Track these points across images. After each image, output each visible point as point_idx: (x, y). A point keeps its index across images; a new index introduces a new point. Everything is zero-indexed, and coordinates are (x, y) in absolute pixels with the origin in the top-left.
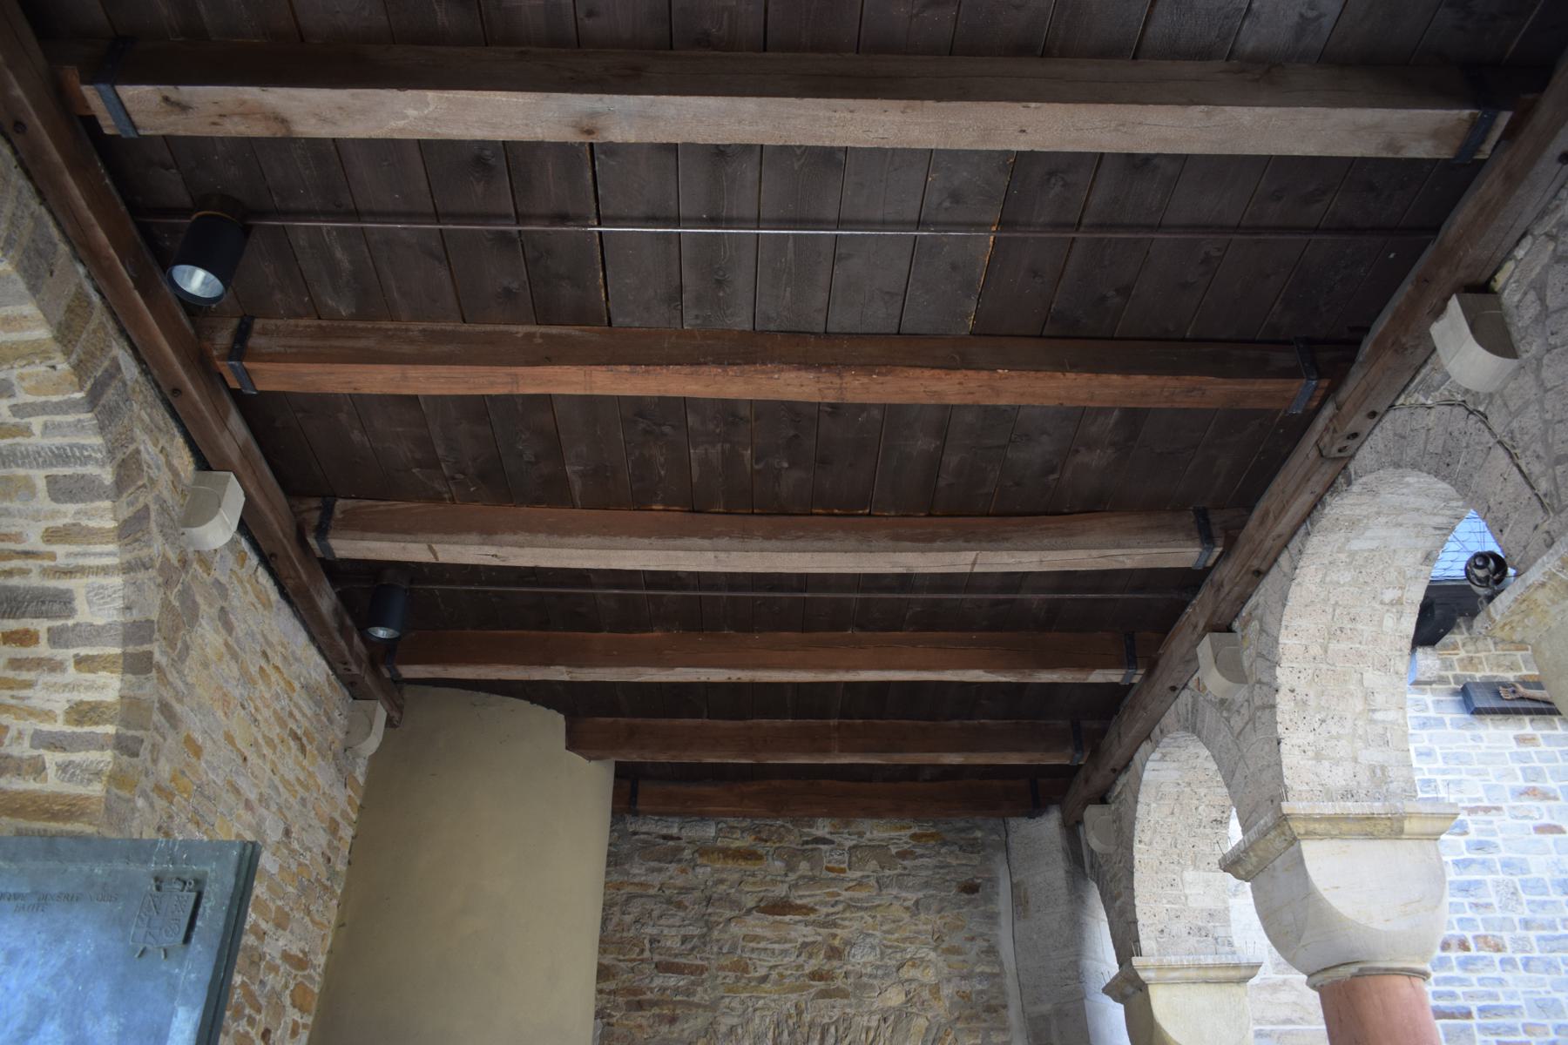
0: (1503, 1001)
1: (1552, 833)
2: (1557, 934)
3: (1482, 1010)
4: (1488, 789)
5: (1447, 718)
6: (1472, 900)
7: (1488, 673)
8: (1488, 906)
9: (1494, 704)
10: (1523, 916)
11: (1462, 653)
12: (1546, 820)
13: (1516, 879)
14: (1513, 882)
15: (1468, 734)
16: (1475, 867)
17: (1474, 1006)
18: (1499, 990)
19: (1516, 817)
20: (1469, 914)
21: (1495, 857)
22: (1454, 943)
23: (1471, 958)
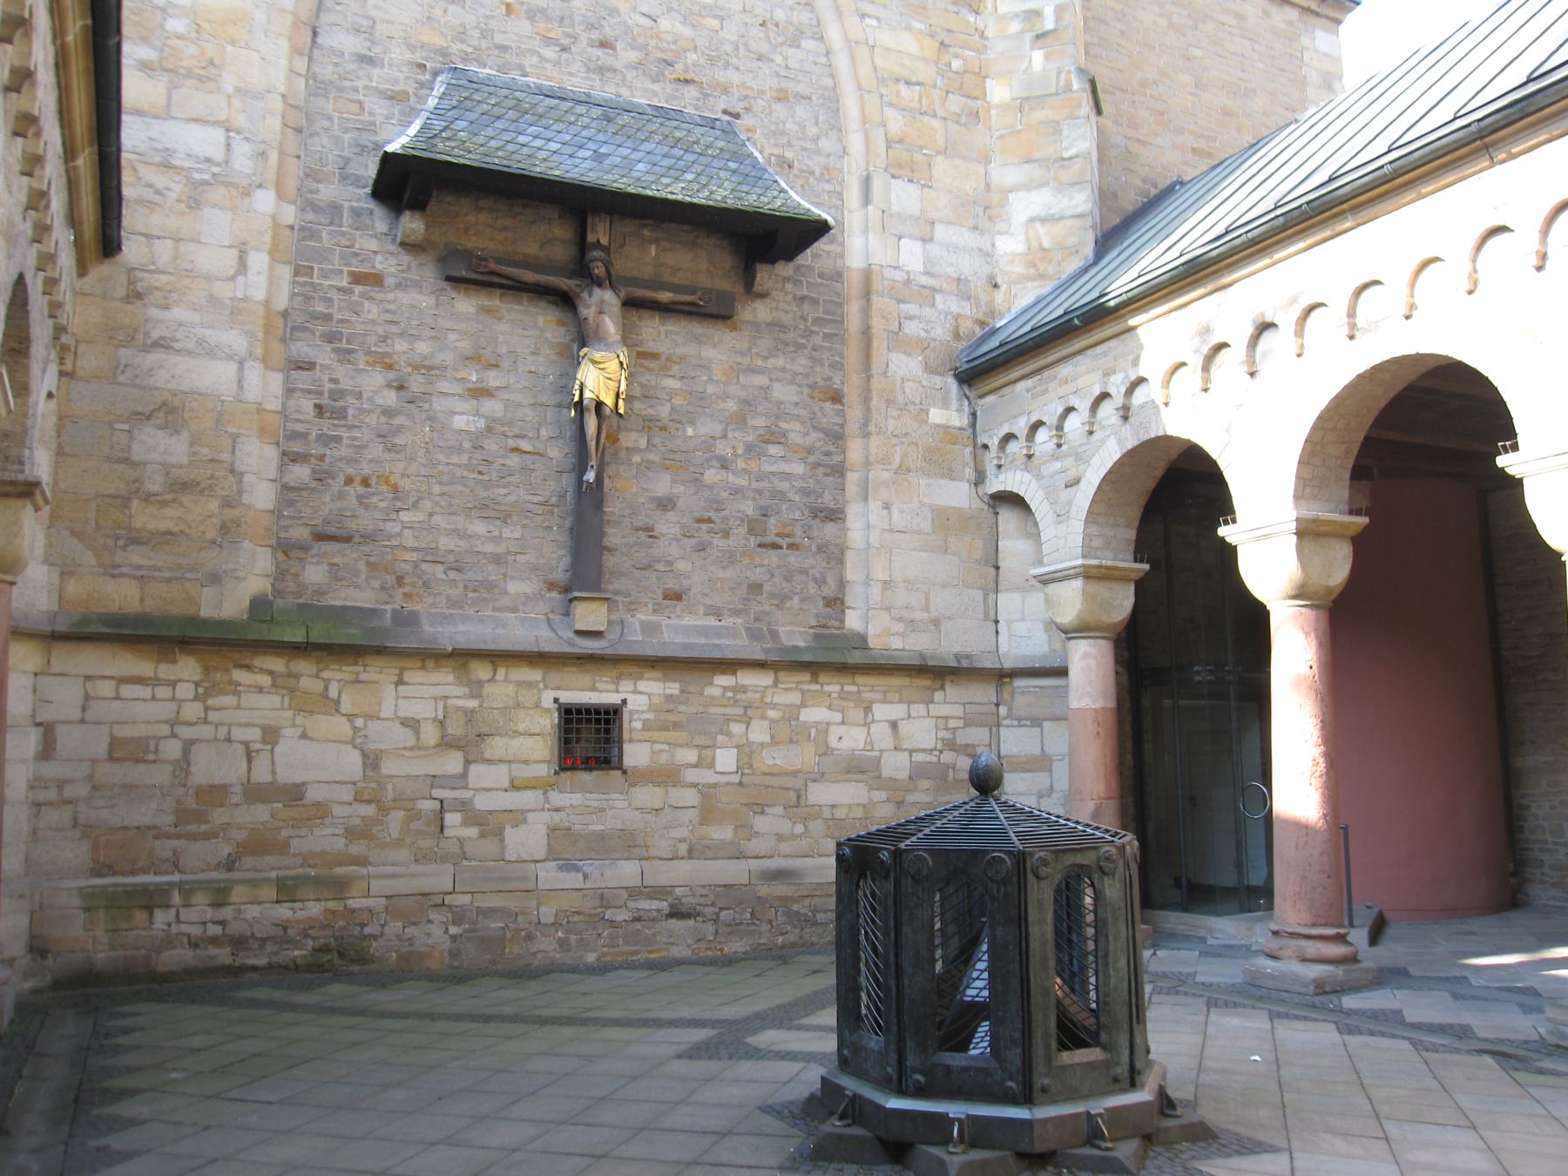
9: (472, 276)
22: (358, 479)
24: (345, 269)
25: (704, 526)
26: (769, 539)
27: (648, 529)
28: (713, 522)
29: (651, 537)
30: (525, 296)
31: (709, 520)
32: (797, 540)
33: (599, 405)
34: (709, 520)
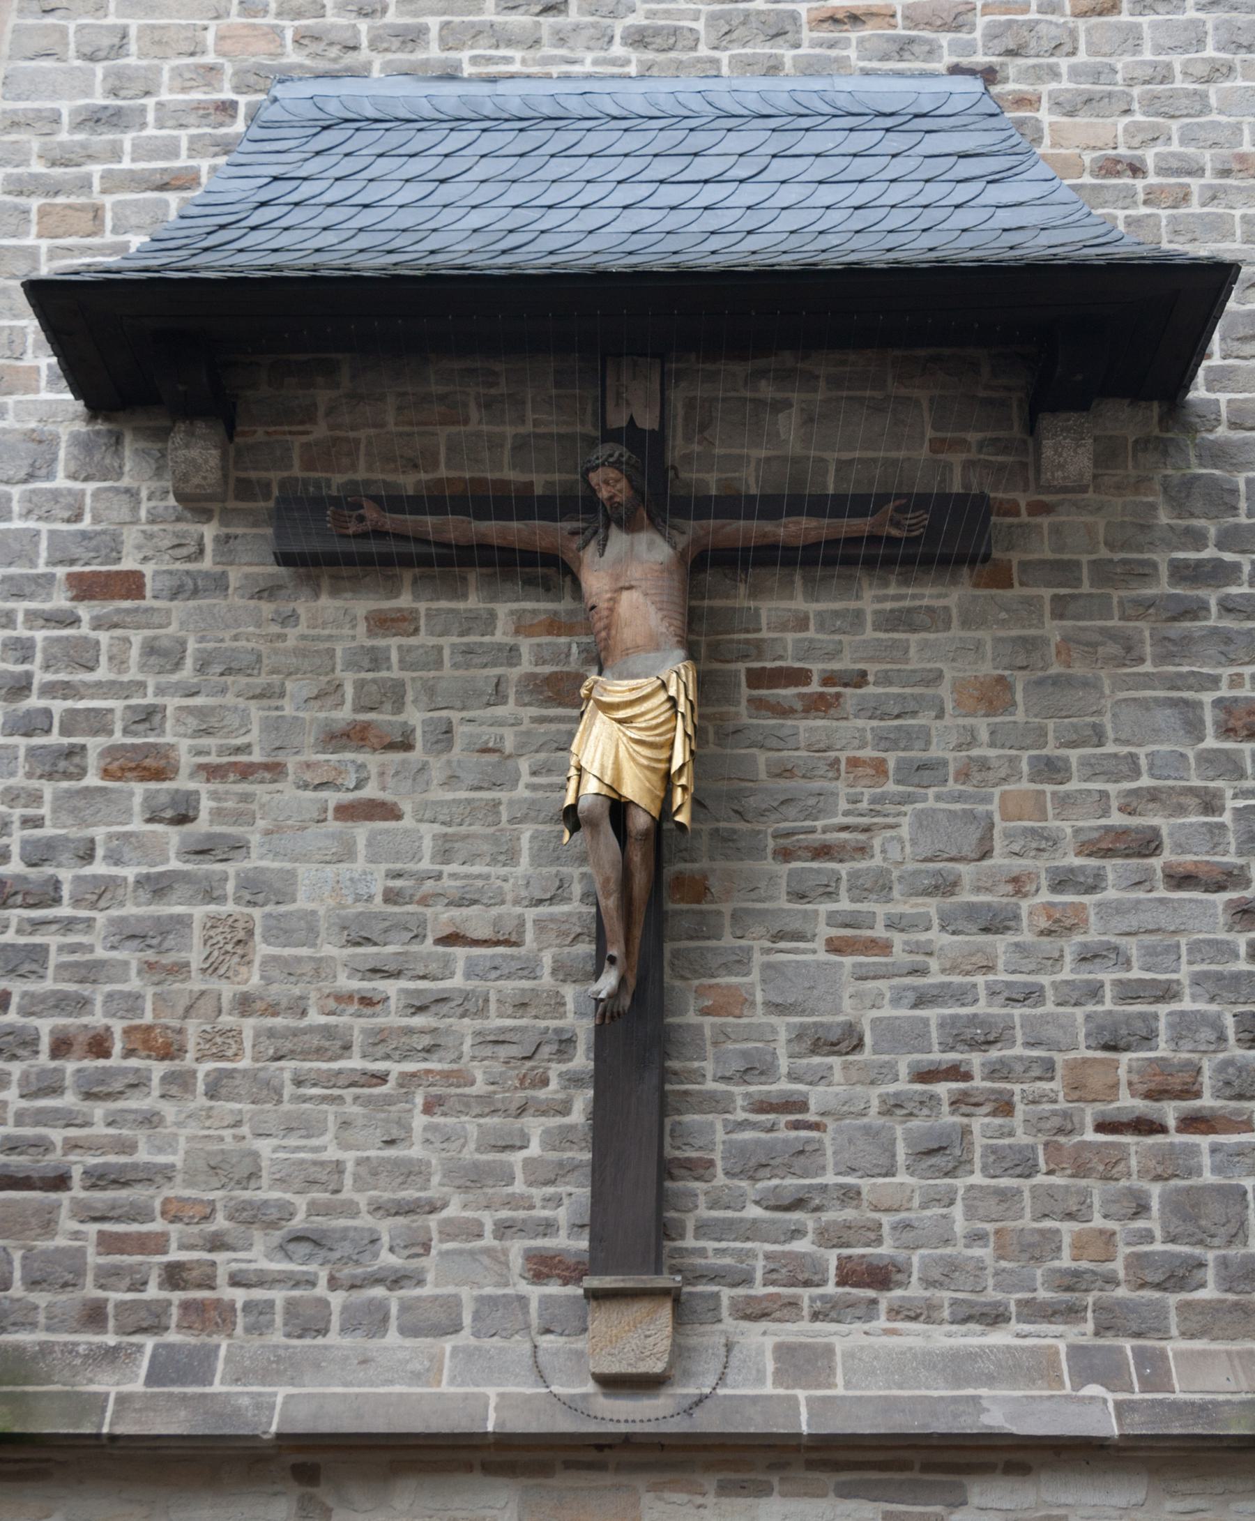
0: (143, 1155)
1: (370, 817)
2: (304, 1023)
3: (99, 1179)
4: (272, 726)
5: (235, 576)
6: (150, 955)
7: (361, 475)
8: (180, 969)
10: (244, 988)
11: (320, 431)
12: (370, 791)
13: (257, 913)
14: (251, 917)
15: (267, 608)
16: (181, 890)
17: (78, 1164)
18: (141, 1136)
19: (306, 786)
20: (134, 984)
21: (230, 868)
23: (105, 1070)
24: (61, 571)
25: (943, 1089)
26: (1128, 1103)
27: (795, 1105)
28: (967, 1077)
29: (796, 1126)
30: (473, 576)
31: (955, 1072)
32: (1207, 1101)
33: (618, 809)
34: (955, 1072)
